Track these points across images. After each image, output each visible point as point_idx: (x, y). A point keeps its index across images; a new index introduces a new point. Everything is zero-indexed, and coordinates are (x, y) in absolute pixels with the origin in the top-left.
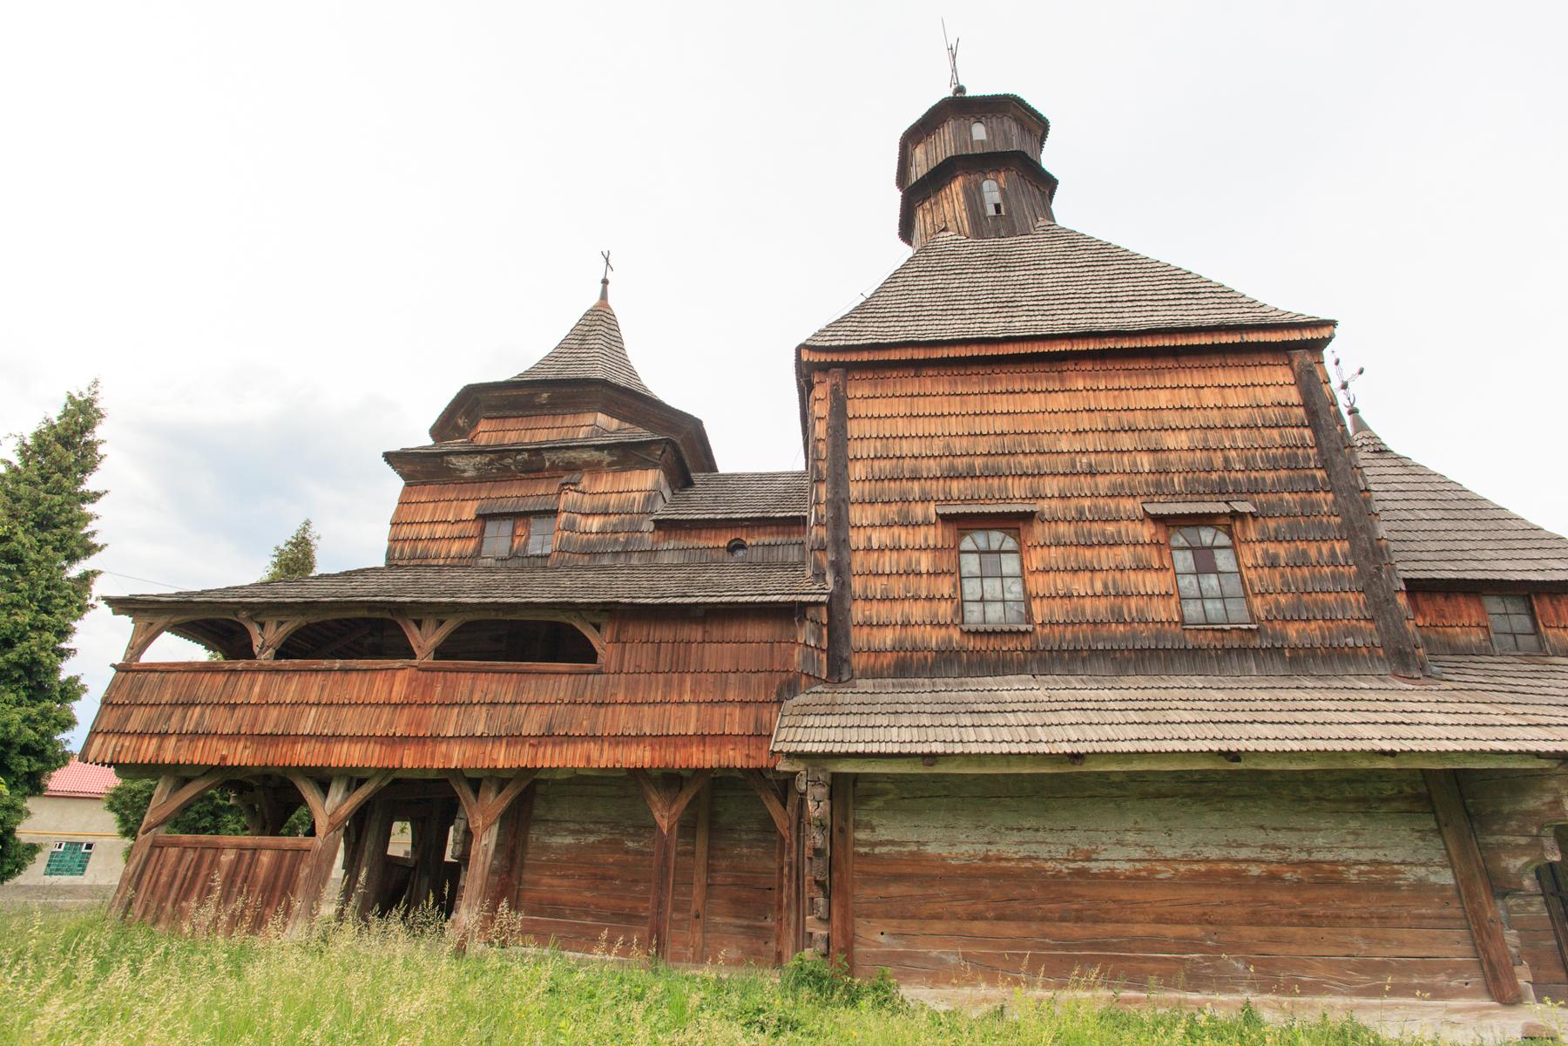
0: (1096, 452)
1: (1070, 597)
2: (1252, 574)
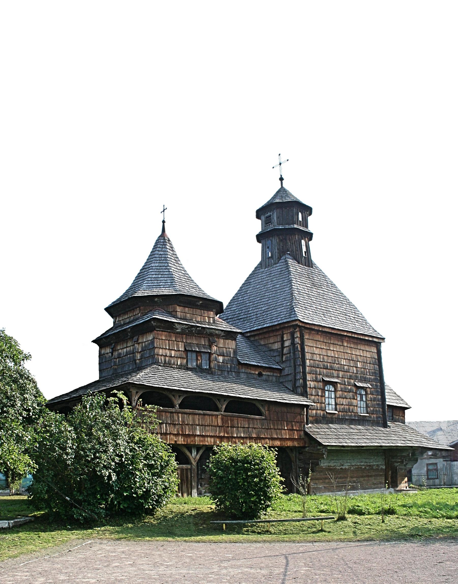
1: (342, 405)
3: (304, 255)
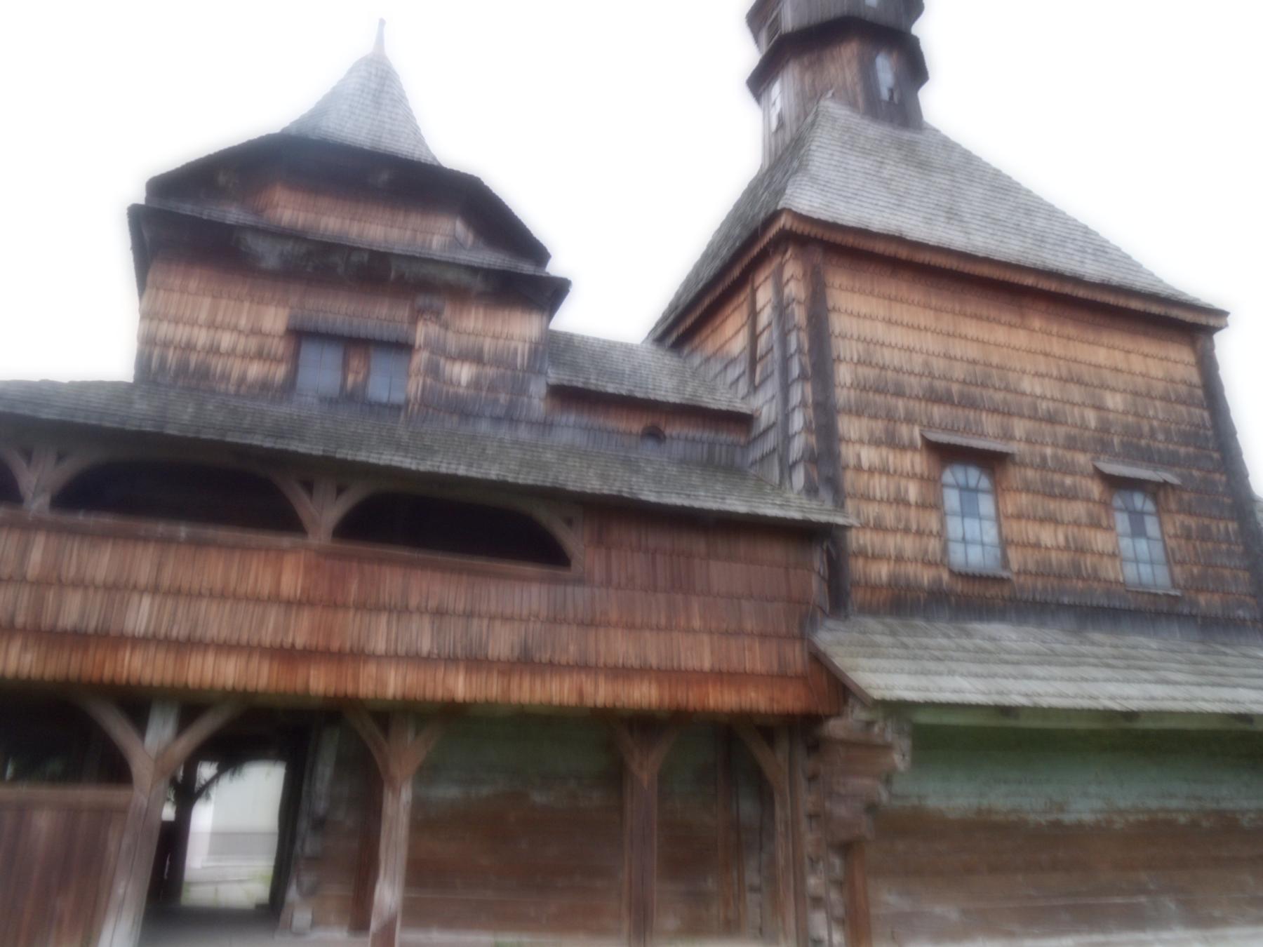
0: (1053, 399)
2: (1172, 543)
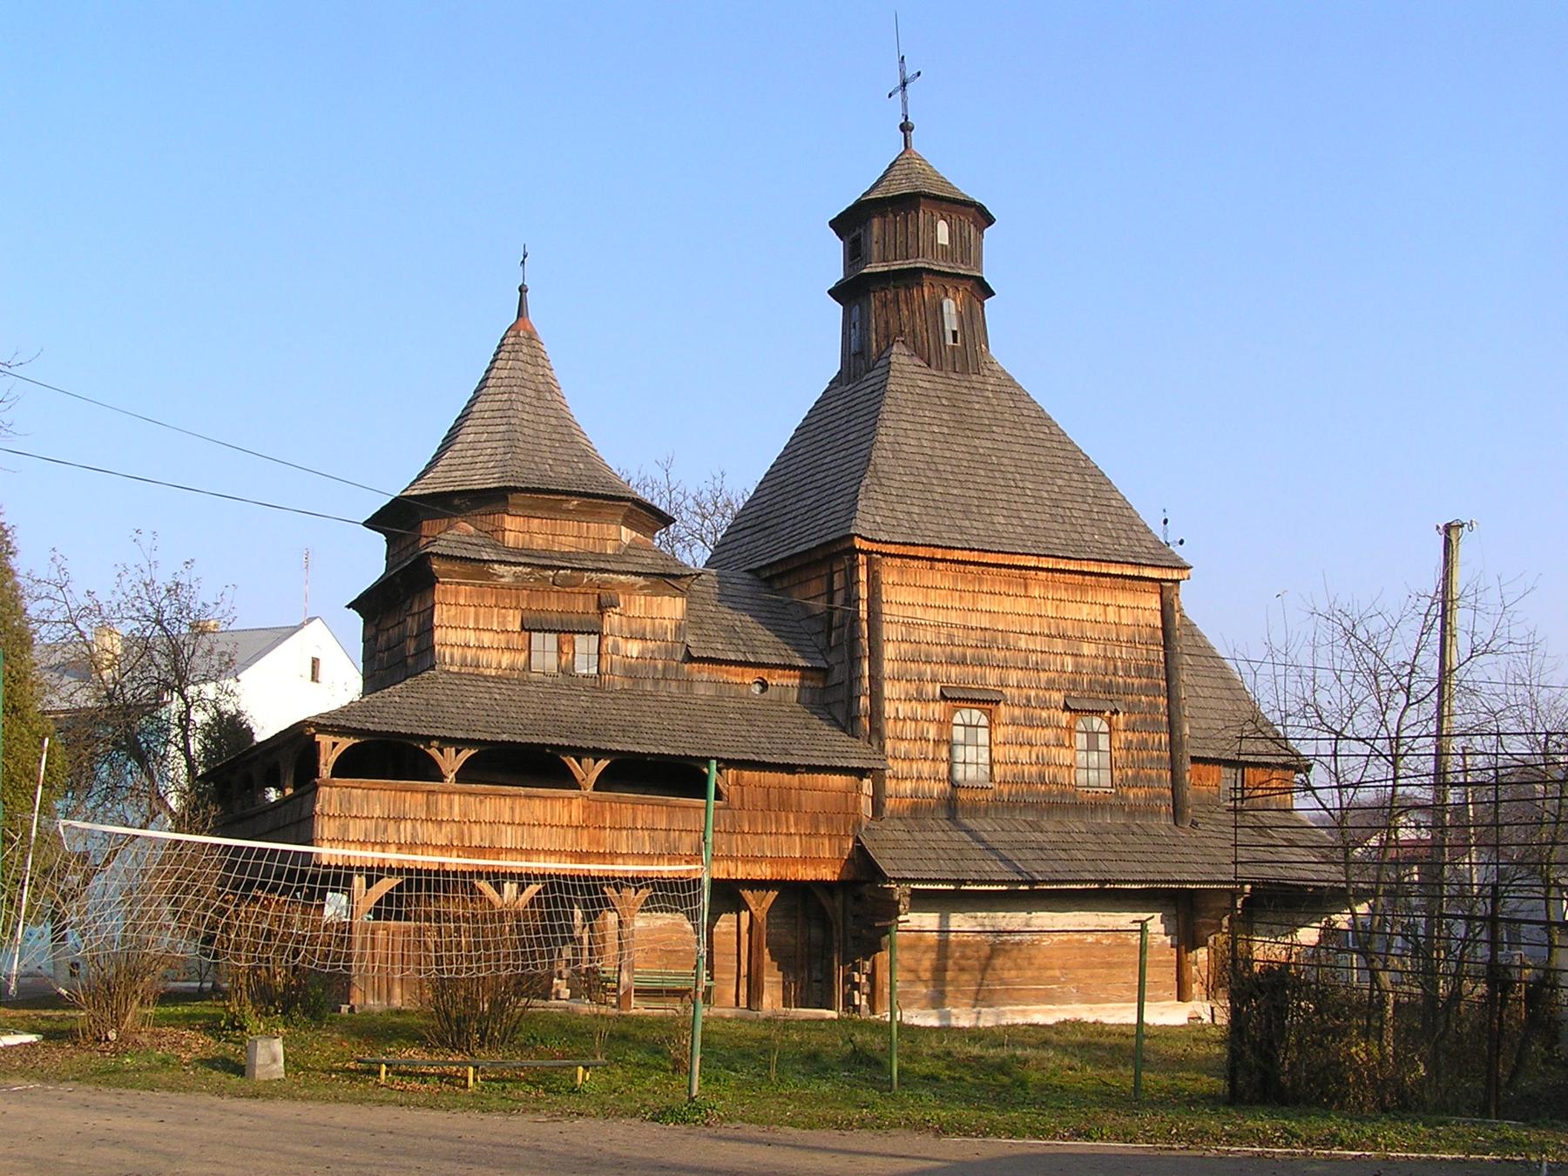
1: (1016, 763)
3: (950, 342)
